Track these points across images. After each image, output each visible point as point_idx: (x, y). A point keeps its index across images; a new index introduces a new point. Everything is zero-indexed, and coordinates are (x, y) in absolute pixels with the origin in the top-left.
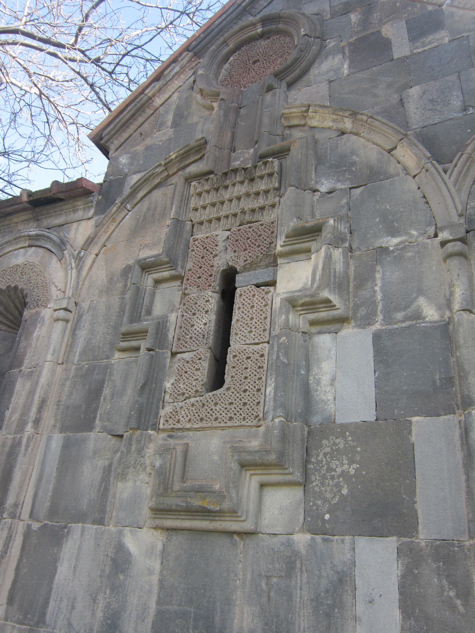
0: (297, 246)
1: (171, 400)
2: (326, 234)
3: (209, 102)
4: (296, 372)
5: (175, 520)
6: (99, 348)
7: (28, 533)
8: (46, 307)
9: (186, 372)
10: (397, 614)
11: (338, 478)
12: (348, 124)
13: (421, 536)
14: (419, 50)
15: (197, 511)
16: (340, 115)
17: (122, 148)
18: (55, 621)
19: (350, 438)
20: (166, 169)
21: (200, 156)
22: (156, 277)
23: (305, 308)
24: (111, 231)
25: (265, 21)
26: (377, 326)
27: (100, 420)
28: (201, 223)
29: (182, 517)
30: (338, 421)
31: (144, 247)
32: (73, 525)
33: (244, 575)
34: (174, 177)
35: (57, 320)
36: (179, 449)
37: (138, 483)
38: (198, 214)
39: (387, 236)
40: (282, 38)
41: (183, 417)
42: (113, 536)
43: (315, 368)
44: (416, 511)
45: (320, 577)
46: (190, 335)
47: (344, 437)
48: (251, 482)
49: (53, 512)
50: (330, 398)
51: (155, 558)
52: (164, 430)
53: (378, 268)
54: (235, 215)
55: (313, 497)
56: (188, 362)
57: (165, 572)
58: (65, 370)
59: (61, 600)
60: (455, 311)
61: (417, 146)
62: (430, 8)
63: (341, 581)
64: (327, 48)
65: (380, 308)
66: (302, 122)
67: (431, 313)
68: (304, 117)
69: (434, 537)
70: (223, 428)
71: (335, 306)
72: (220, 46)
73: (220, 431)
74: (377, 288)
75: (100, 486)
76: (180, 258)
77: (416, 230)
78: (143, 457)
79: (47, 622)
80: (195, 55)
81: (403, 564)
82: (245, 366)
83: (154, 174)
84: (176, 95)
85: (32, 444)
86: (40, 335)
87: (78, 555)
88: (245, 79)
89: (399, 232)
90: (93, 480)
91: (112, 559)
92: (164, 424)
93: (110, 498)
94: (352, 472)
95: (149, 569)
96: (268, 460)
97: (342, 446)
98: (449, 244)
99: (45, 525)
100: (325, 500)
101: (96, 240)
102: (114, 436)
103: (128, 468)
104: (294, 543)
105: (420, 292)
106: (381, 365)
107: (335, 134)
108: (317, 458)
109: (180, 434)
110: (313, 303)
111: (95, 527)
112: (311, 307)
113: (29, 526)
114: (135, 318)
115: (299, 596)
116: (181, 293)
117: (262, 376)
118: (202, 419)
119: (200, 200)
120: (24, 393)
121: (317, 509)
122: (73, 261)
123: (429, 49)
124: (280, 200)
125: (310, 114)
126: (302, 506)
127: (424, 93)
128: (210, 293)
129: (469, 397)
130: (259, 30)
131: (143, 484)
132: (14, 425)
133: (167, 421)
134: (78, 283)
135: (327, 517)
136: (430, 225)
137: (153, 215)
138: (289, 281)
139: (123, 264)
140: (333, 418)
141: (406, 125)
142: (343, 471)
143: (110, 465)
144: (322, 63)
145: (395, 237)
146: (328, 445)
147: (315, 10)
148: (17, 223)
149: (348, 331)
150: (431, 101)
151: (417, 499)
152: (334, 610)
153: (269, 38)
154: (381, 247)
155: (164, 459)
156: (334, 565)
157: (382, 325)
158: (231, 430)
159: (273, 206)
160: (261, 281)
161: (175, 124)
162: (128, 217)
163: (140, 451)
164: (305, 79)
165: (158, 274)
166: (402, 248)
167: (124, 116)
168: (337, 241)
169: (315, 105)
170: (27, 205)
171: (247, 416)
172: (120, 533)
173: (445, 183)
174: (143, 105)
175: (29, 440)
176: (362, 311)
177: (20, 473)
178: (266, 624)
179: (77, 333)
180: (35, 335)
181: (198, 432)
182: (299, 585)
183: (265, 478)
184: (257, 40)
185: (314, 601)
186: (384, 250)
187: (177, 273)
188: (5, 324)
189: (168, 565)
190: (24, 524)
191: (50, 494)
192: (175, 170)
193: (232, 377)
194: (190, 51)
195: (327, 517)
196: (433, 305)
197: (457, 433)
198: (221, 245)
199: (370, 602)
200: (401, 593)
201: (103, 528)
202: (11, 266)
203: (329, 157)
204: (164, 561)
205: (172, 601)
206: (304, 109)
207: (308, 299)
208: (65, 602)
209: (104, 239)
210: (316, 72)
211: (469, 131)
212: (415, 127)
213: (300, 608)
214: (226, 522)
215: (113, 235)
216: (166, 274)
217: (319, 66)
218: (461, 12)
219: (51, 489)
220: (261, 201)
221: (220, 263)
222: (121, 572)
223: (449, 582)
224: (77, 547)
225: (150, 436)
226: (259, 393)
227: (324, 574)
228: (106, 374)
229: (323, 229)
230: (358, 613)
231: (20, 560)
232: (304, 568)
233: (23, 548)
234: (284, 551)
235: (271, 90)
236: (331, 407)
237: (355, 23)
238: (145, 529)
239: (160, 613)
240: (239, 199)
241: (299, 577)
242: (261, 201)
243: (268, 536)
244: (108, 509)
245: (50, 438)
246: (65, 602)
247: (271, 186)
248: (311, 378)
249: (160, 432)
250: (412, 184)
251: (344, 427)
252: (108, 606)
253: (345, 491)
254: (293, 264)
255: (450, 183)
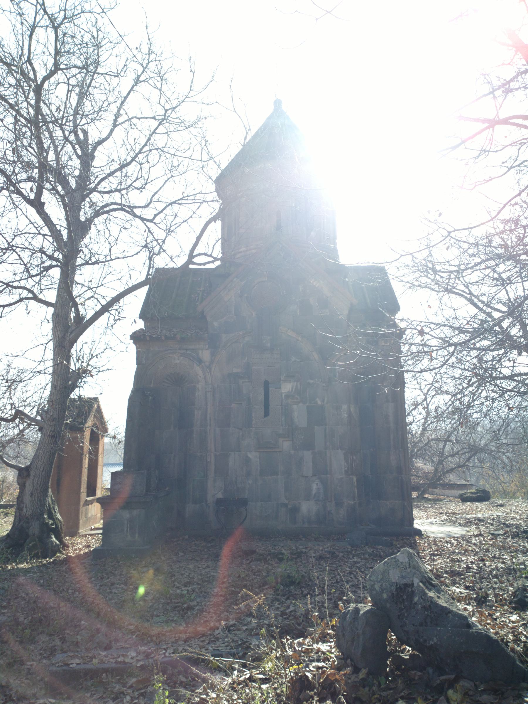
12: (300, 339)
26: (307, 404)
149: (301, 404)
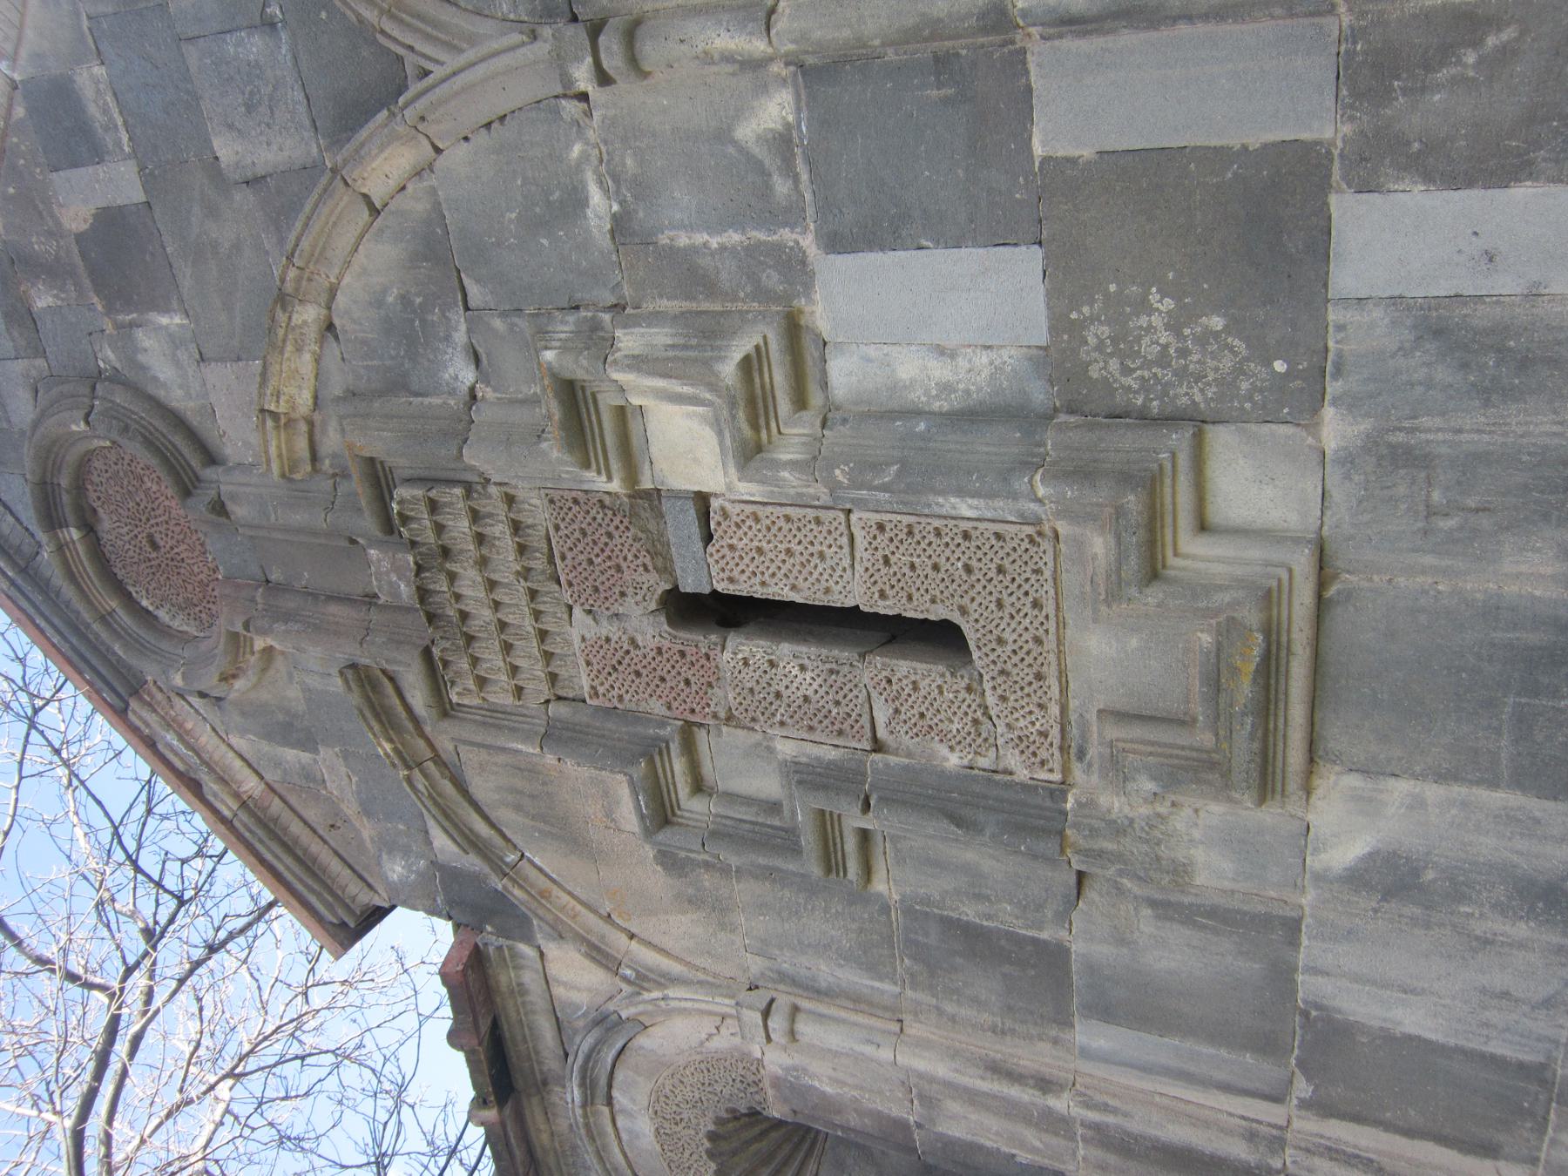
0: (610, 440)
1: (992, 753)
2: (579, 368)
3: (253, 659)
4: (923, 445)
5: (1289, 742)
6: (861, 930)
7: (1321, 1107)
8: (760, 1062)
9: (922, 715)
10: (1521, 193)
11: (1185, 338)
12: (308, 315)
13: (1328, 134)
14: (125, 138)
15: (1267, 688)
16: (286, 335)
17: (366, 875)
18: (1538, 1040)
19: (1086, 310)
20: (419, 765)
21: (386, 681)
22: (687, 790)
23: (762, 421)
24: (573, 902)
25: (51, 519)
26: (808, 242)
27: (1040, 929)
28: (553, 678)
29: (1281, 726)
30: (1042, 338)
31: (613, 820)
32: (1300, 995)
33: (1423, 572)
34: (438, 745)
35: (792, 1034)
36: (1113, 732)
37: (1196, 834)
38: (529, 686)
39: (585, 217)
40: (96, 479)
41: (1033, 723)
42: (1327, 895)
43: (912, 396)
44: (1265, 146)
45: (1429, 384)
46: (831, 706)
47: (1082, 324)
48: (1195, 555)
49: (1268, 1045)
50: (985, 360)
51: (1382, 791)
52: (1066, 770)
53: (663, 239)
54: (533, 594)
55: (1231, 401)
56: (897, 711)
57: (1418, 769)
58: (916, 1014)
59: (1486, 1025)
60: (770, 50)
61: (362, 145)
62: (20, 112)
63: (1438, 333)
64: (118, 366)
65: (761, 236)
66: (303, 427)
67: (776, 109)
68: (290, 423)
69: (1330, 102)
70: (1061, 624)
71: (757, 348)
72: (115, 631)
73: (1068, 632)
74: (714, 243)
75: (1204, 927)
76: (640, 729)
77: (569, 147)
78: (1132, 821)
79: (1542, 1059)
80: (135, 692)
81: (1398, 179)
82: (906, 570)
83: (430, 795)
84: (235, 740)
85: (1099, 1098)
86: (830, 1078)
87: (1374, 983)
88: (196, 569)
89: (575, 188)
90: (1188, 945)
91: (1384, 899)
92: (1051, 770)
93: (1235, 904)
94: (1168, 303)
95: (1411, 807)
96: (1139, 513)
97: (1105, 330)
98: (605, 65)
99: (1301, 1063)
100: (1239, 371)
101: (594, 940)
102: (1079, 894)
103: (1158, 859)
104: (1346, 448)
105: (723, 135)
106: (904, 233)
107: (333, 349)
108: (1136, 392)
109: (1074, 732)
110: (751, 402)
111: (1305, 941)
112: (761, 405)
113: (1304, 1104)
114: (787, 842)
115: (1476, 437)
116: (724, 729)
117: (930, 528)
118: (1039, 677)
119: (496, 682)
120: (973, 1117)
121: (1261, 391)
122: (646, 996)
123: (121, 113)
124: (496, 484)
125: (282, 408)
126: (1253, 427)
127: (231, 127)
128: (727, 655)
129: (982, 16)
130: (75, 534)
131: (1200, 822)
132: (1054, 1141)
133: (1043, 763)
134: (700, 983)
135: (1280, 366)
136: (556, 112)
137: (532, 797)
138: (695, 460)
139: (654, 872)
140: (1034, 352)
141: (309, 172)
142: (1167, 327)
143: (1153, 903)
144: (155, 379)
145: (587, 199)
146: (1102, 364)
147: (24, 395)
148: (552, 1134)
149: (820, 315)
150: (250, 108)
151: (1236, 143)
152: (1510, 350)
153: (95, 511)
154: (612, 231)
155: (1137, 770)
156: (1400, 349)
157: (805, 231)
158: (1065, 605)
159: (510, 500)
160: (695, 530)
161: (308, 742)
162: (537, 860)
163: (1119, 829)
164: (195, 421)
165: (679, 786)
166: (614, 180)
167: (288, 868)
168: (597, 342)
169: (261, 395)
170: (507, 1111)
171: (1031, 565)
172: (1320, 878)
173: (454, 74)
174: (259, 821)
175: (1089, 1104)
176: (772, 279)
177: (1171, 1127)
178: (1546, 517)
179: (824, 985)
180: (828, 1090)
181: (1071, 685)
182: (1449, 436)
183: (1185, 520)
184: (98, 539)
185: (1488, 400)
186: (620, 227)
187: (677, 738)
188: (803, 1163)
189: (1400, 759)
190: (1299, 1117)
191: (1223, 1053)
192: (421, 743)
193: (933, 601)
194: (127, 705)
195: (1280, 366)
196: (756, 104)
197: (1071, 44)
198: (607, 628)
199: (1491, 260)
200: (1470, 184)
201: (1307, 921)
202: (658, 1148)
203: (388, 363)
204: (1388, 770)
205: (1489, 751)
206: (270, 423)
207: (741, 415)
208: (1492, 1016)
209: (591, 919)
210: (180, 393)
211: (324, 15)
212: (315, 150)
213: (1506, 434)
214: (1294, 617)
215: (583, 897)
216: (679, 765)
217: (164, 385)
218: (29, 33)
219: (1212, 1051)
220: (499, 530)
221: (649, 629)
222: (1418, 877)
223: (1442, 64)
224: (1356, 986)
225: (1079, 804)
226: (974, 534)
227: (1422, 373)
228: (927, 913)
229: (568, 375)
230: (1518, 291)
231: (1388, 1126)
232: (1406, 424)
233: (1358, 1119)
234: (1365, 474)
235: (223, 505)
236: (1009, 357)
237: (56, 296)
238: (1310, 817)
239: (1520, 781)
240: (492, 585)
241: (1430, 437)
242: (499, 530)
243: (1328, 513)
244: (1261, 908)
245: (1085, 1053)
246: (1492, 1016)
247: (461, 505)
248: (936, 406)
249: (1070, 780)
250: (457, 157)
251: (1058, 323)
252: (1501, 909)
253: (1217, 322)
254: (654, 450)
255: (452, 62)
